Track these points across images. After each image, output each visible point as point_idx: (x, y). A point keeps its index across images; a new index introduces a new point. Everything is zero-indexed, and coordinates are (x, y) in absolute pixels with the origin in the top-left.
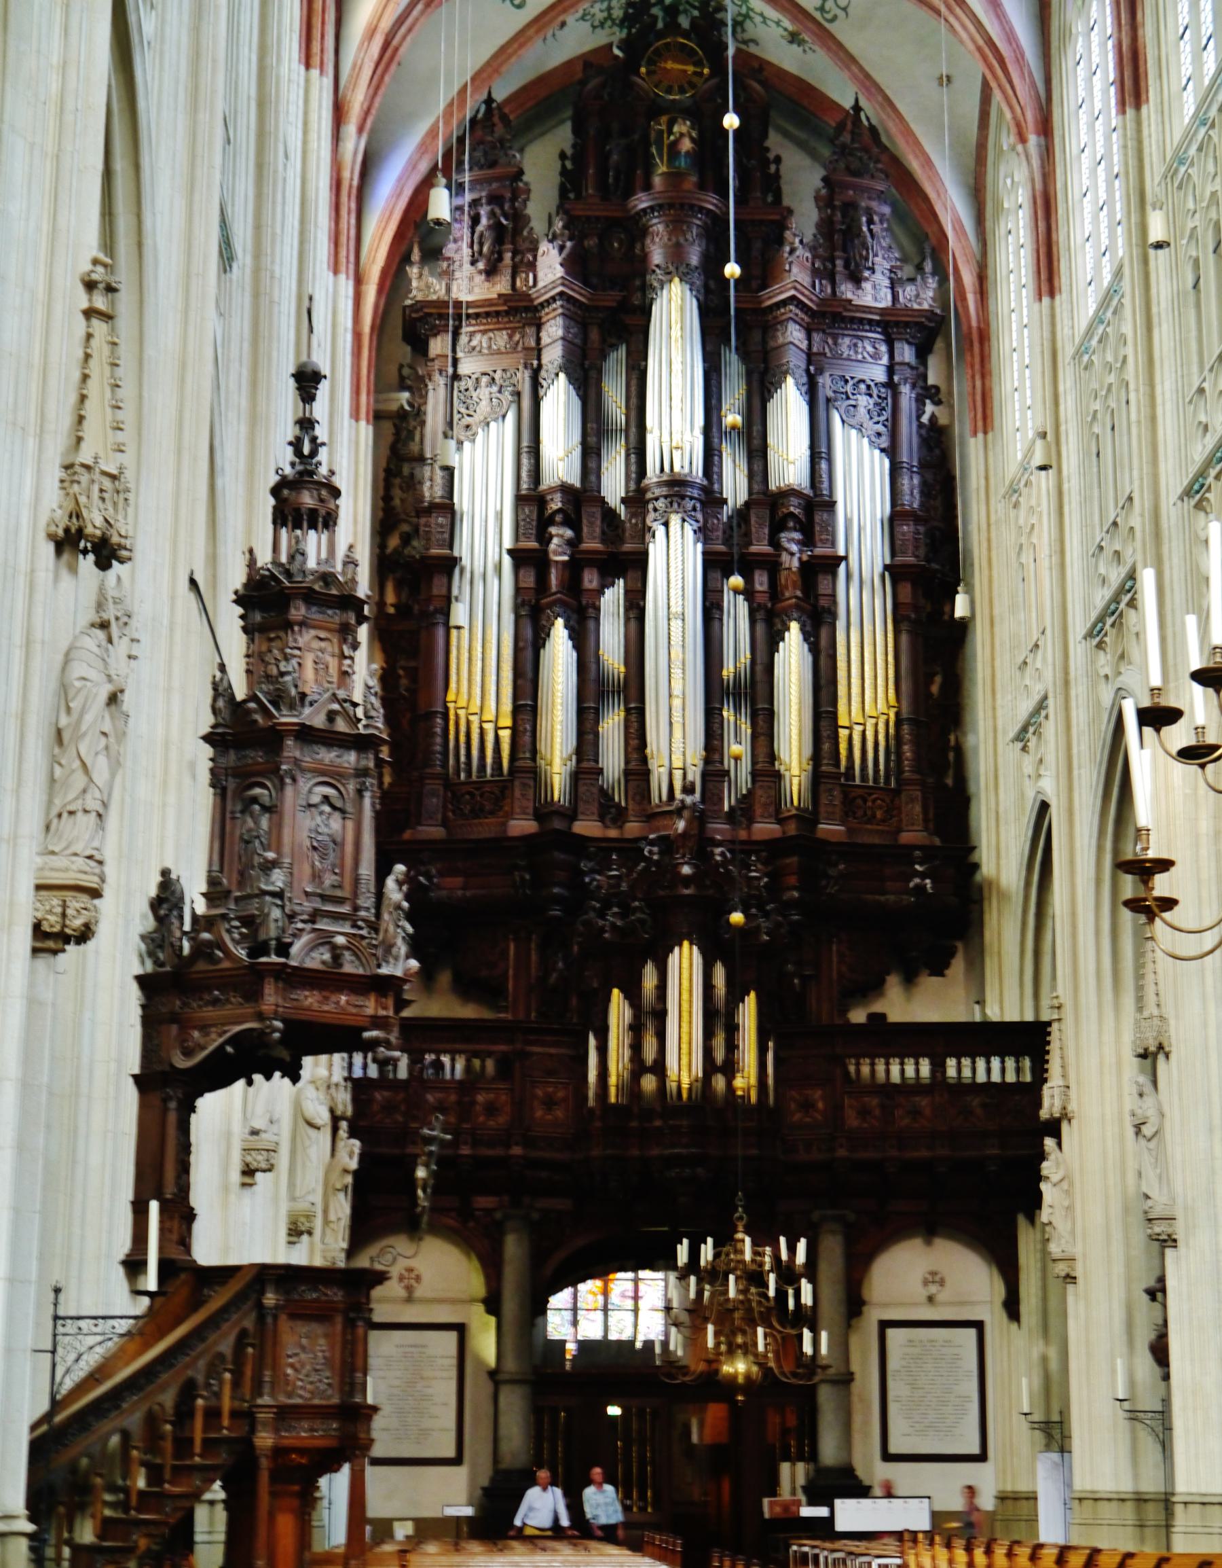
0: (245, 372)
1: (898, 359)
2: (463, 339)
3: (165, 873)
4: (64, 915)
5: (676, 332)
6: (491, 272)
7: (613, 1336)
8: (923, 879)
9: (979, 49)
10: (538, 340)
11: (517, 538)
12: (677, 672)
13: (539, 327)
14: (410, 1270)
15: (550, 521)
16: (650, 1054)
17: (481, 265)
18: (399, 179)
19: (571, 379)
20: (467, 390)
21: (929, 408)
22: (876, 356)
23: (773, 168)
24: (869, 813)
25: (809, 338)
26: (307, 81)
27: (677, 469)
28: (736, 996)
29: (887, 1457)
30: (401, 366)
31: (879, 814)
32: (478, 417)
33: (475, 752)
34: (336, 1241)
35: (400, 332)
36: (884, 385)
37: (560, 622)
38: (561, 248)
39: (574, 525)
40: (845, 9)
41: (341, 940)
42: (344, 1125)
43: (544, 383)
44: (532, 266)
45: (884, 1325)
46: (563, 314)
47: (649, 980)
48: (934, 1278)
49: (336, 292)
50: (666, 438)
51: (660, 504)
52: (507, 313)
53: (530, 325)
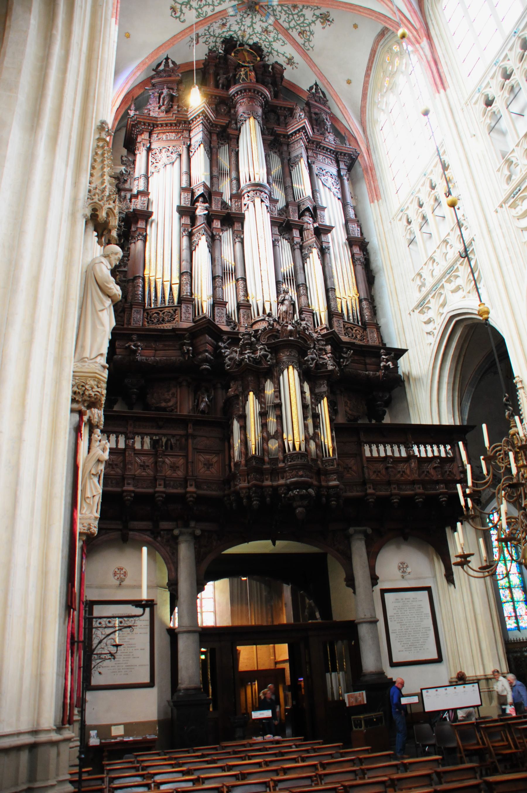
2: (155, 136)
8: (387, 362)
10: (189, 136)
13: (190, 131)
15: (197, 201)
16: (272, 428)
17: (163, 108)
18: (127, 78)
20: (156, 154)
24: (354, 335)
29: (393, 665)
30: (122, 157)
31: (358, 336)
34: (91, 512)
35: (122, 144)
40: (312, 48)
43: (193, 151)
45: (383, 591)
46: (202, 123)
47: (269, 390)
48: (403, 567)
53: (186, 130)
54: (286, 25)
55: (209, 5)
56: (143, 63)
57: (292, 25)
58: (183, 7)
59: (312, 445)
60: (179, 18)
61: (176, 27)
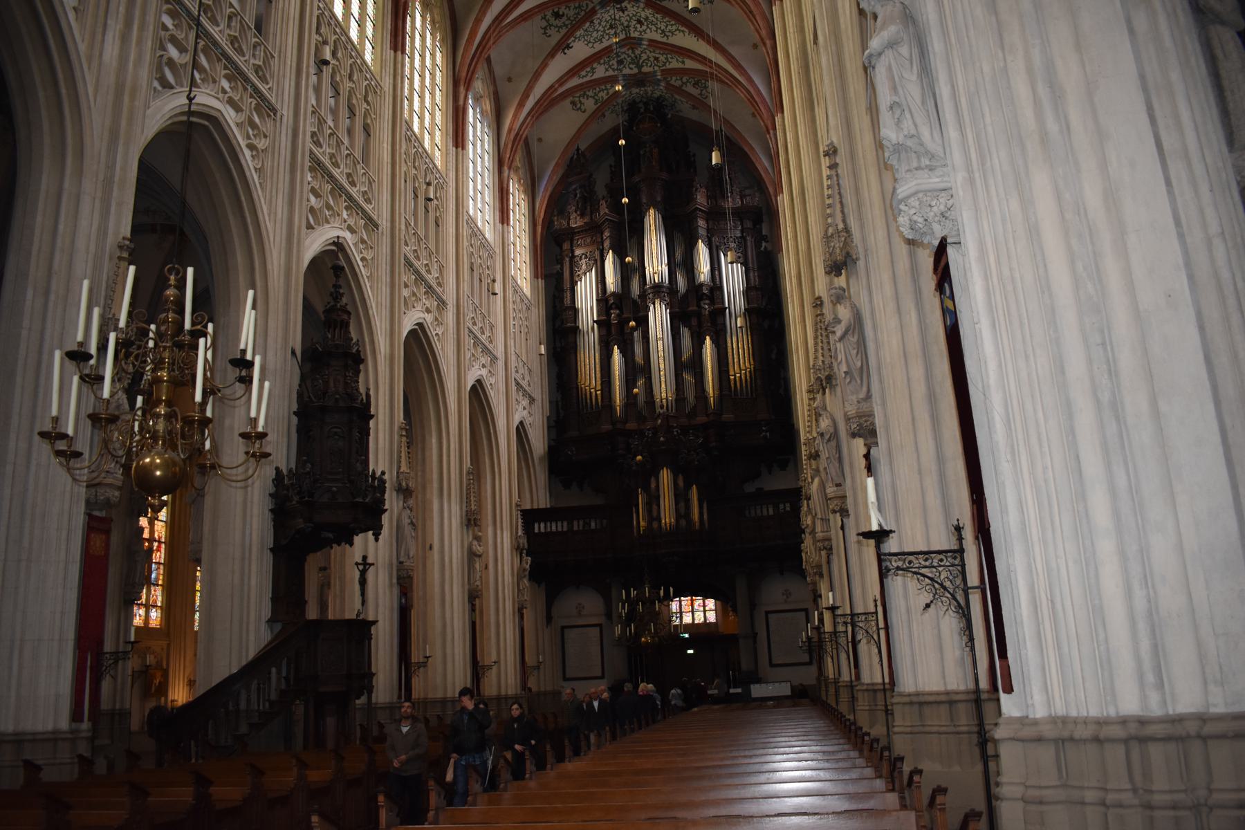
0: (388, 268)
1: (745, 226)
3: (277, 469)
4: (96, 495)
5: (653, 228)
6: (582, 215)
7: (696, 622)
9: (749, 100)
10: (602, 238)
11: (598, 316)
12: (661, 361)
13: (602, 234)
14: (580, 604)
15: (611, 308)
16: (655, 514)
19: (614, 252)
21: (764, 244)
22: (735, 227)
23: (692, 159)
25: (707, 223)
26: (457, 153)
27: (657, 281)
28: (688, 487)
29: (772, 665)
32: (581, 272)
33: (588, 401)
36: (740, 237)
37: (616, 346)
38: (606, 202)
39: (619, 307)
41: (334, 489)
42: (525, 551)
44: (598, 210)
45: (767, 613)
47: (653, 485)
48: (787, 593)
49: (503, 231)
50: (651, 270)
51: (651, 296)
52: (589, 229)
54: (678, 83)
55: (603, 90)
56: (557, 165)
57: (684, 80)
58: (581, 99)
59: (683, 522)
60: (580, 108)
61: (579, 118)
